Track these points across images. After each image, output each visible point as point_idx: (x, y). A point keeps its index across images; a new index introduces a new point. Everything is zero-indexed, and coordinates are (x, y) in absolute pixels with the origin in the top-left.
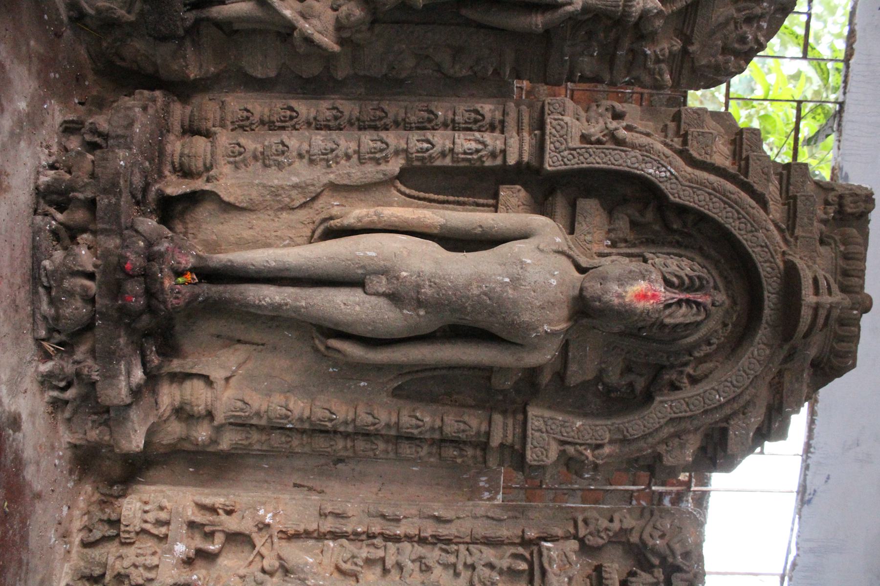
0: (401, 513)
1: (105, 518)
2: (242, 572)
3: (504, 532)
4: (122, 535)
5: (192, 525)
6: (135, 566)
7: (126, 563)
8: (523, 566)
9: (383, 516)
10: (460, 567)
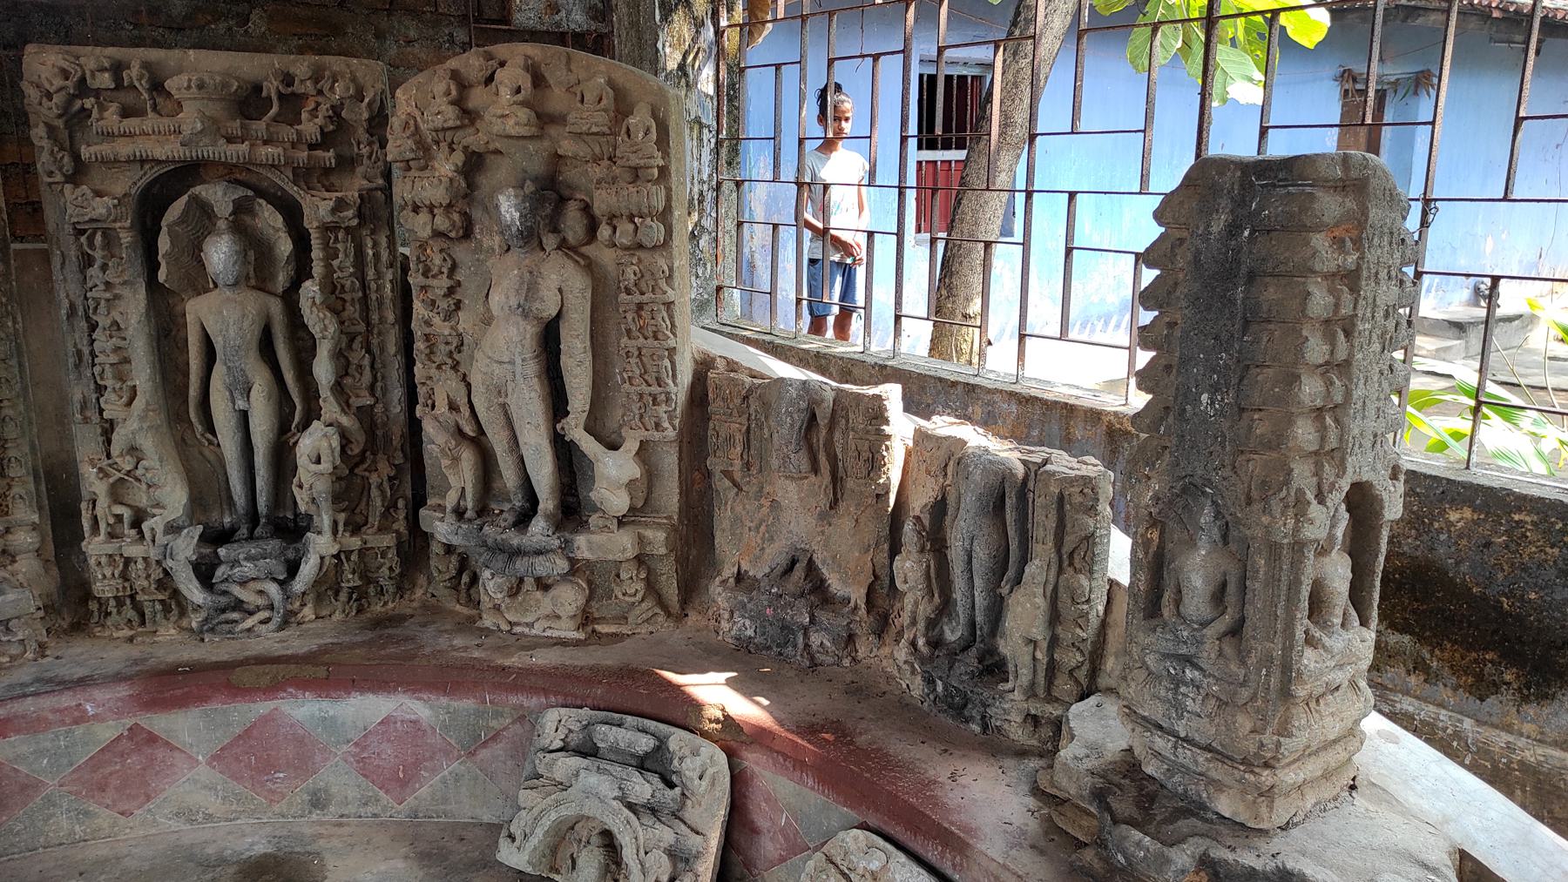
0: (71, 349)
1: (115, 611)
2: (144, 487)
3: (73, 253)
4: (128, 592)
5: (112, 536)
6: (148, 576)
7: (145, 583)
8: (98, 238)
9: (77, 366)
10: (108, 295)
